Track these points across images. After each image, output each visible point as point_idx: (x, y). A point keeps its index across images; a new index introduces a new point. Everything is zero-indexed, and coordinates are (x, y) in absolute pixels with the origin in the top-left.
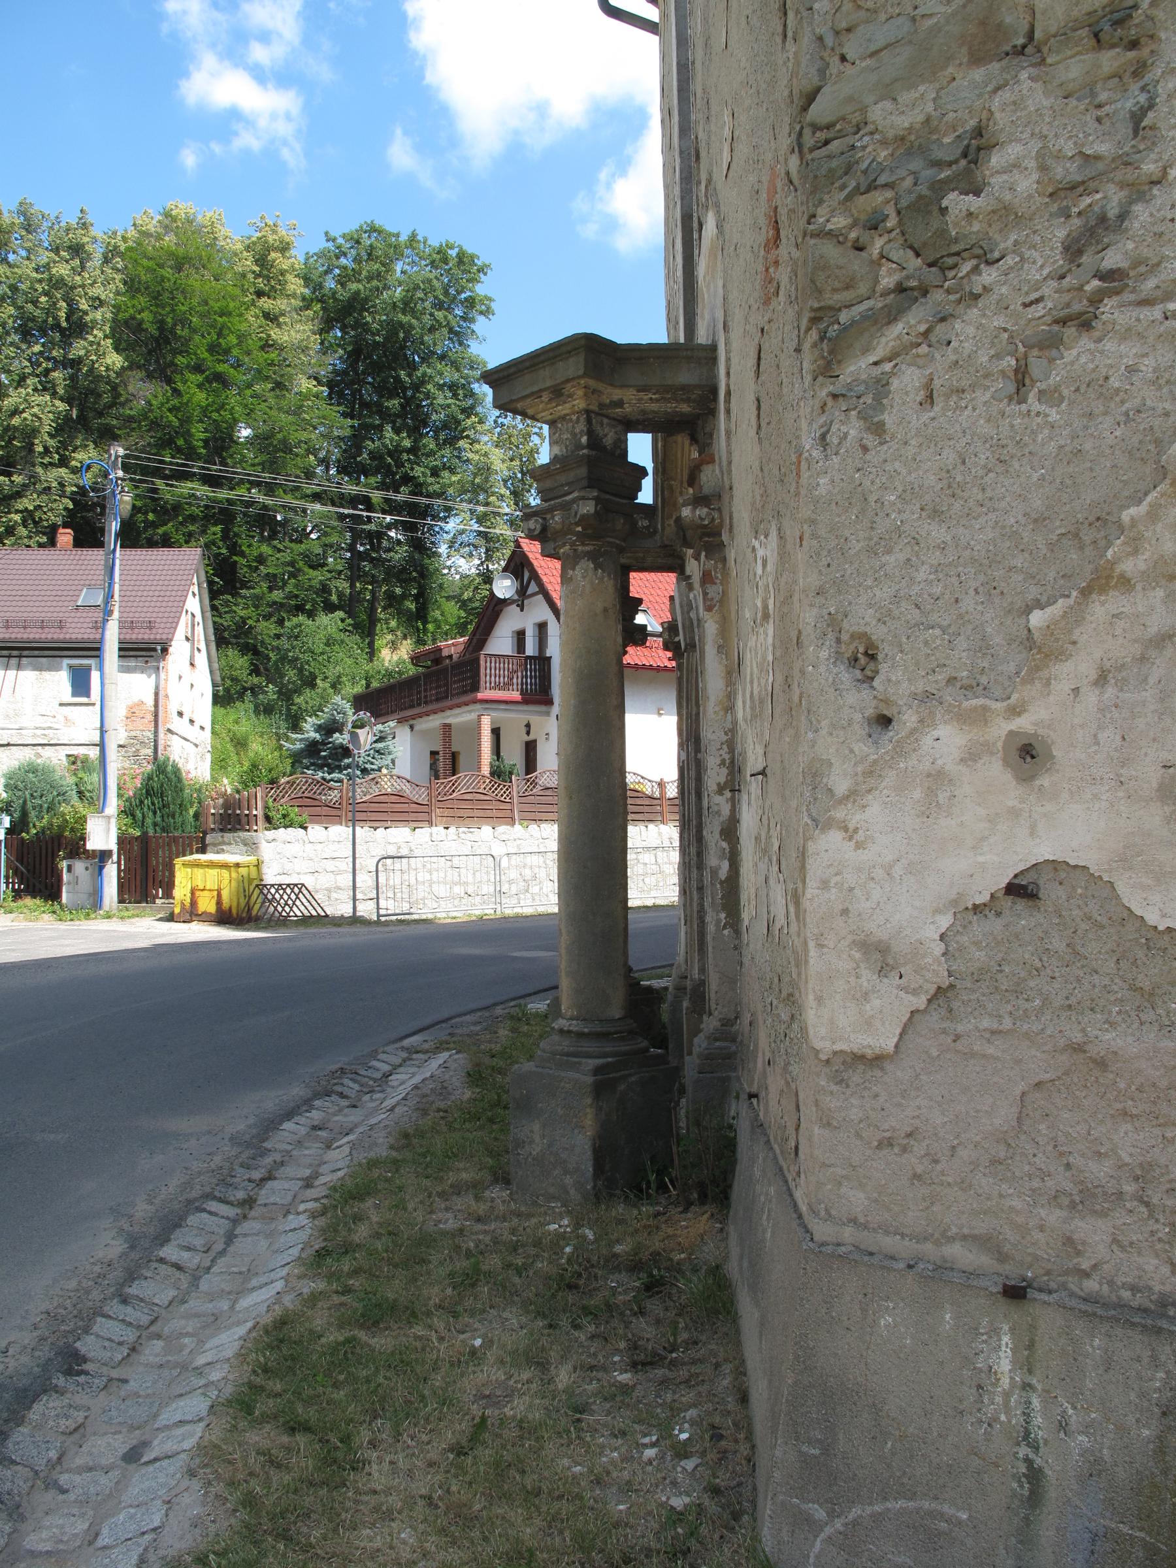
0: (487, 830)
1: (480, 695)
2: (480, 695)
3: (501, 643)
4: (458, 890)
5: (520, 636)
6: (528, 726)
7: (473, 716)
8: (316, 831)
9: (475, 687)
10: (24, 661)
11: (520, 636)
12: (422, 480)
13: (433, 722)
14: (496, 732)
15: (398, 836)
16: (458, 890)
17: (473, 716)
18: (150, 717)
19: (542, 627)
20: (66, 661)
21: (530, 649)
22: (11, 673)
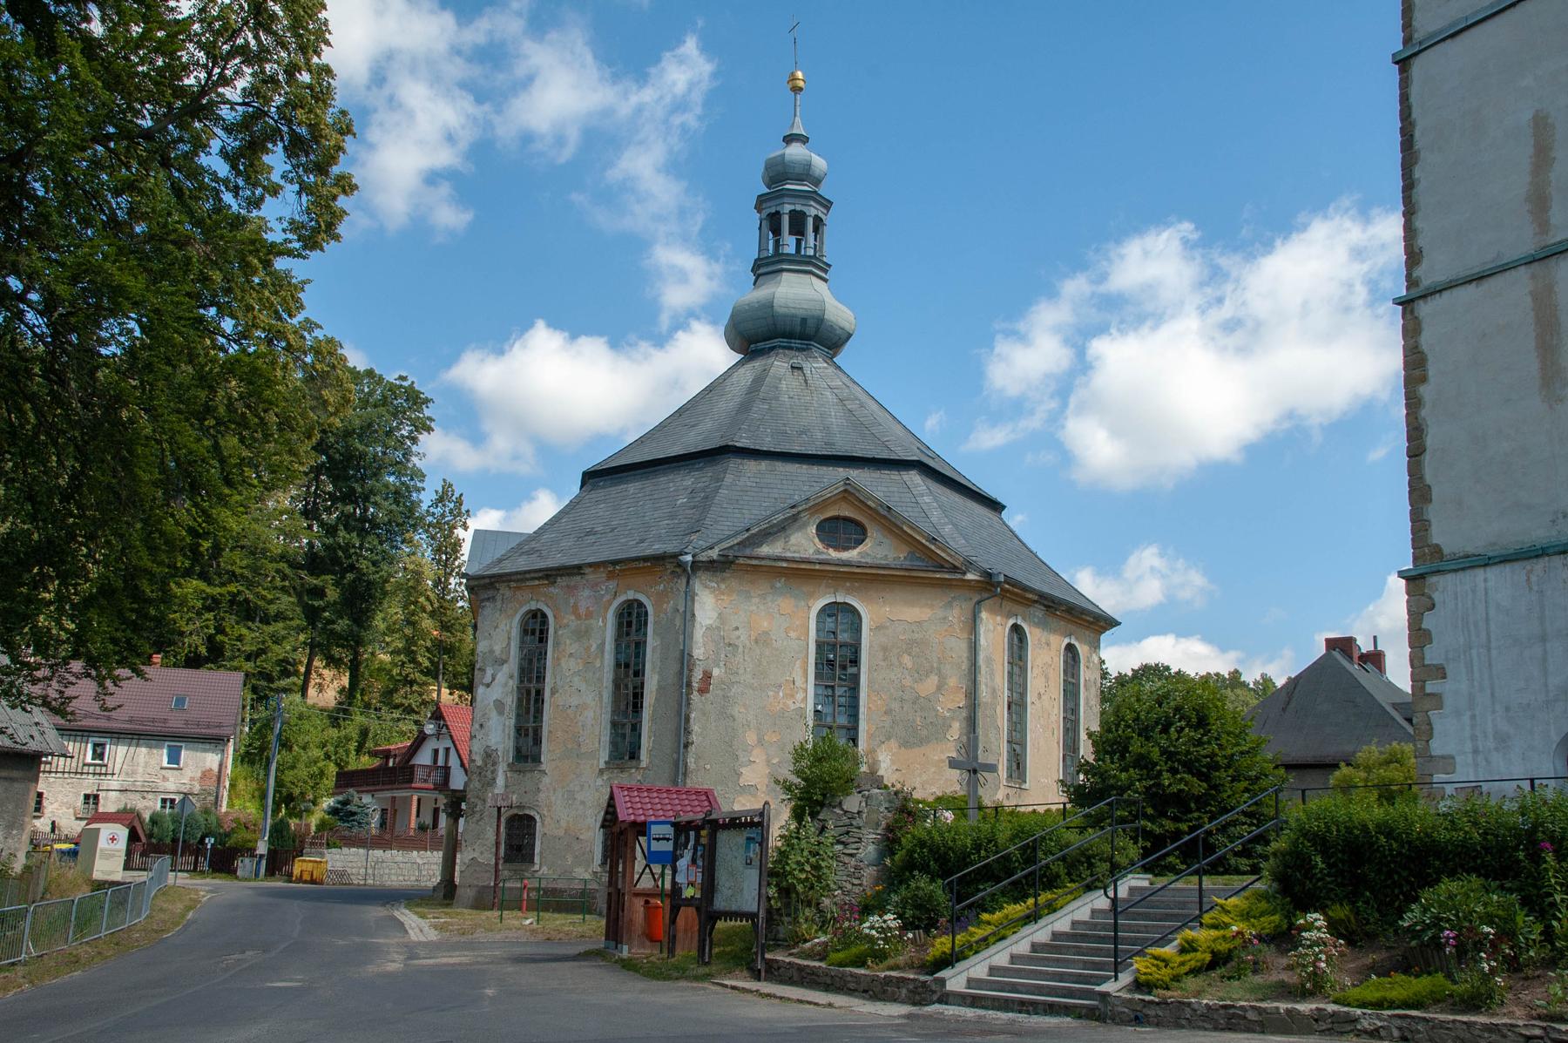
0: (415, 853)
1: (413, 785)
2: (413, 785)
3: (424, 758)
4: (401, 878)
5: (436, 752)
6: (436, 800)
7: (409, 794)
8: (345, 850)
9: (411, 781)
10: (141, 741)
11: (436, 752)
12: (365, 570)
13: (388, 794)
14: (419, 800)
15: (378, 853)
16: (401, 878)
17: (409, 794)
18: (215, 778)
19: (447, 750)
20: (167, 743)
21: (441, 762)
22: (132, 749)
